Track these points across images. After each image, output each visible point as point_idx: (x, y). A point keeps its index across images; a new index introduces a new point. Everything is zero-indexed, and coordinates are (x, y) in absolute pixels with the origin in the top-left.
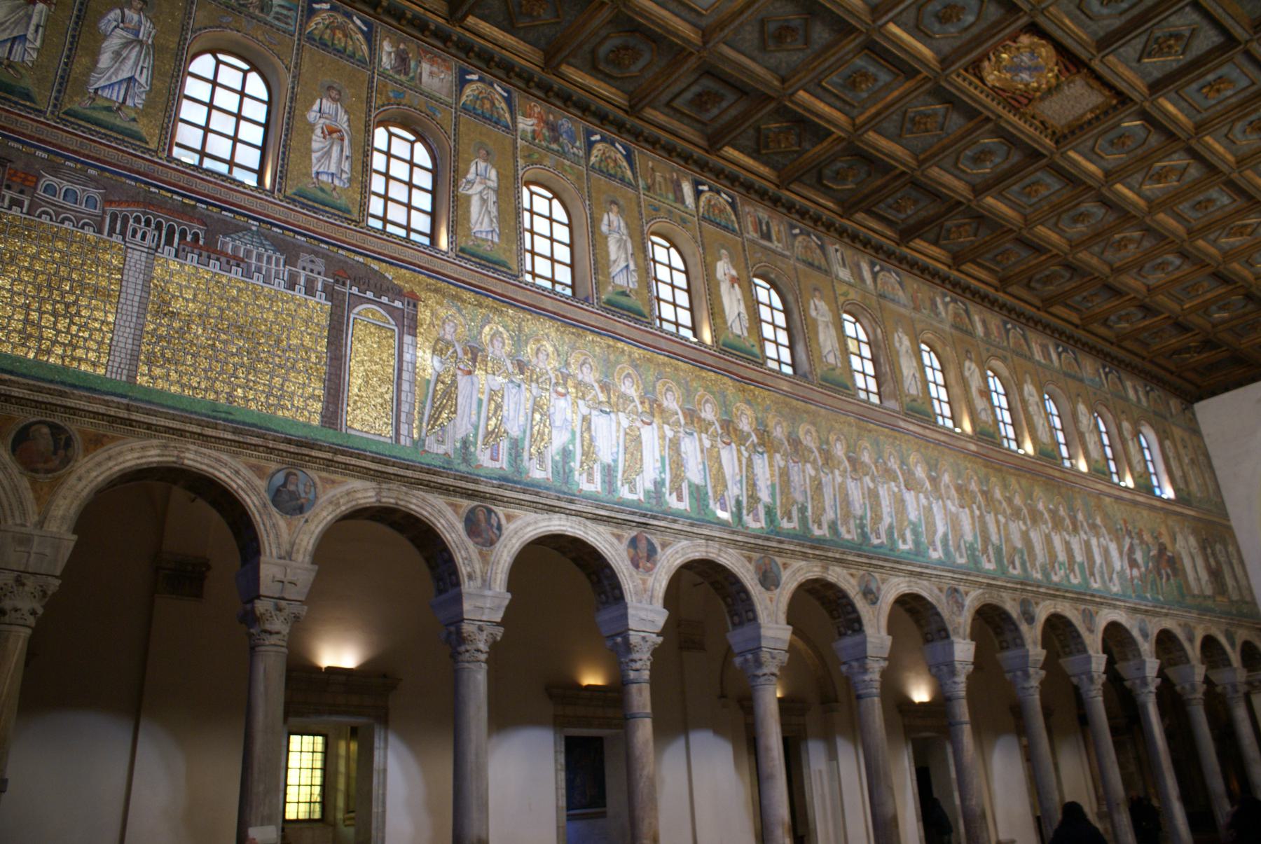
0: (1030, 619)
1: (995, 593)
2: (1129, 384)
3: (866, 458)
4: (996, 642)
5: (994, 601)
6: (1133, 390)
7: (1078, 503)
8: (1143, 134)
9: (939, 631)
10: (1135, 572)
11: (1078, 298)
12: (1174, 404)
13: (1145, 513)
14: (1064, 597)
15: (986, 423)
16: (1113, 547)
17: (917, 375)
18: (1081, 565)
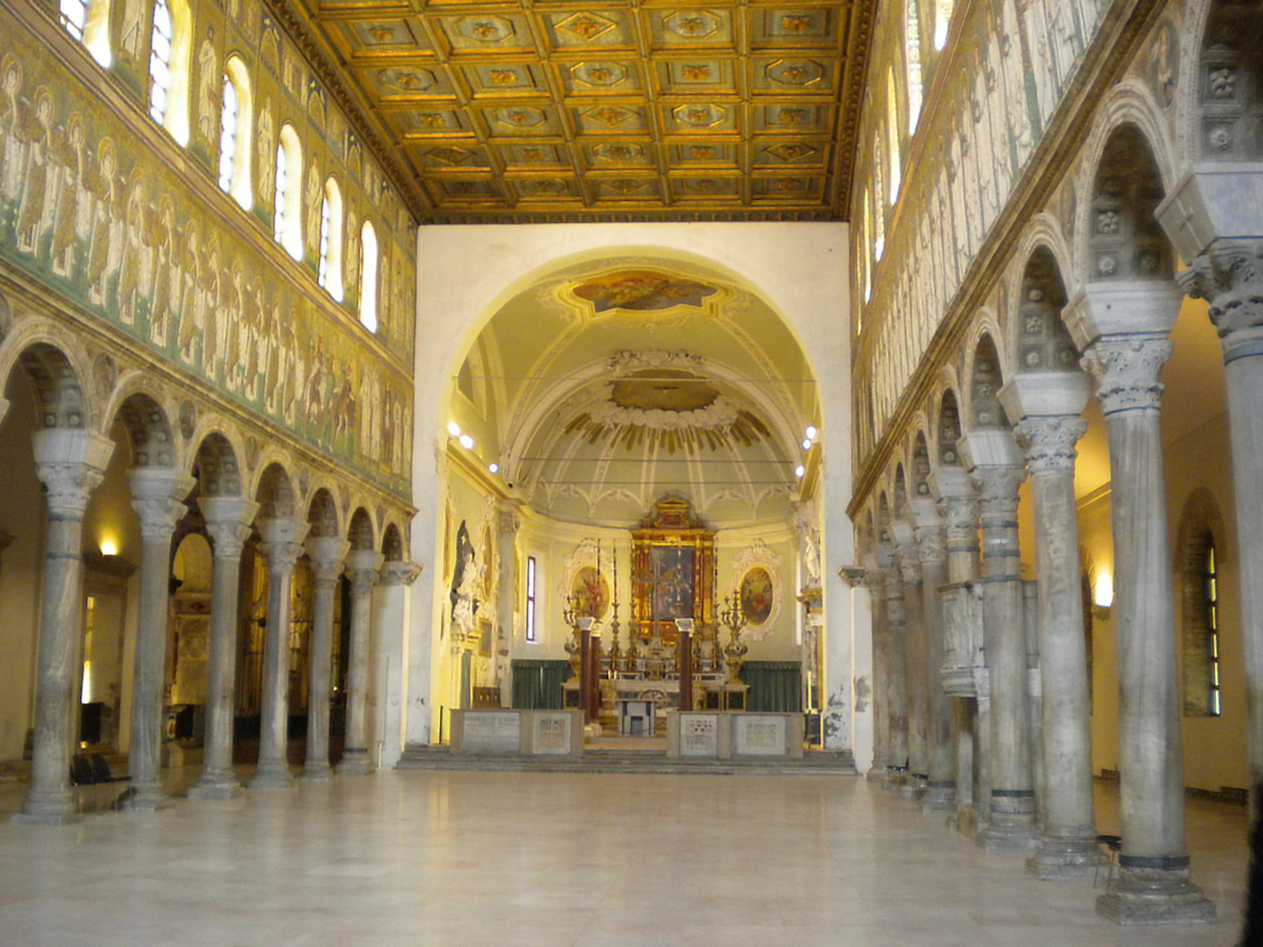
0: (188, 432)
1: (156, 380)
2: (368, 167)
3: (44, 114)
4: (131, 454)
5: (152, 393)
6: (371, 178)
7: (279, 295)
9: (69, 414)
10: (315, 408)
11: (365, 25)
12: (403, 215)
13: (342, 337)
14: (234, 414)
15: (206, 139)
16: (300, 367)
17: (142, 27)
18: (262, 377)
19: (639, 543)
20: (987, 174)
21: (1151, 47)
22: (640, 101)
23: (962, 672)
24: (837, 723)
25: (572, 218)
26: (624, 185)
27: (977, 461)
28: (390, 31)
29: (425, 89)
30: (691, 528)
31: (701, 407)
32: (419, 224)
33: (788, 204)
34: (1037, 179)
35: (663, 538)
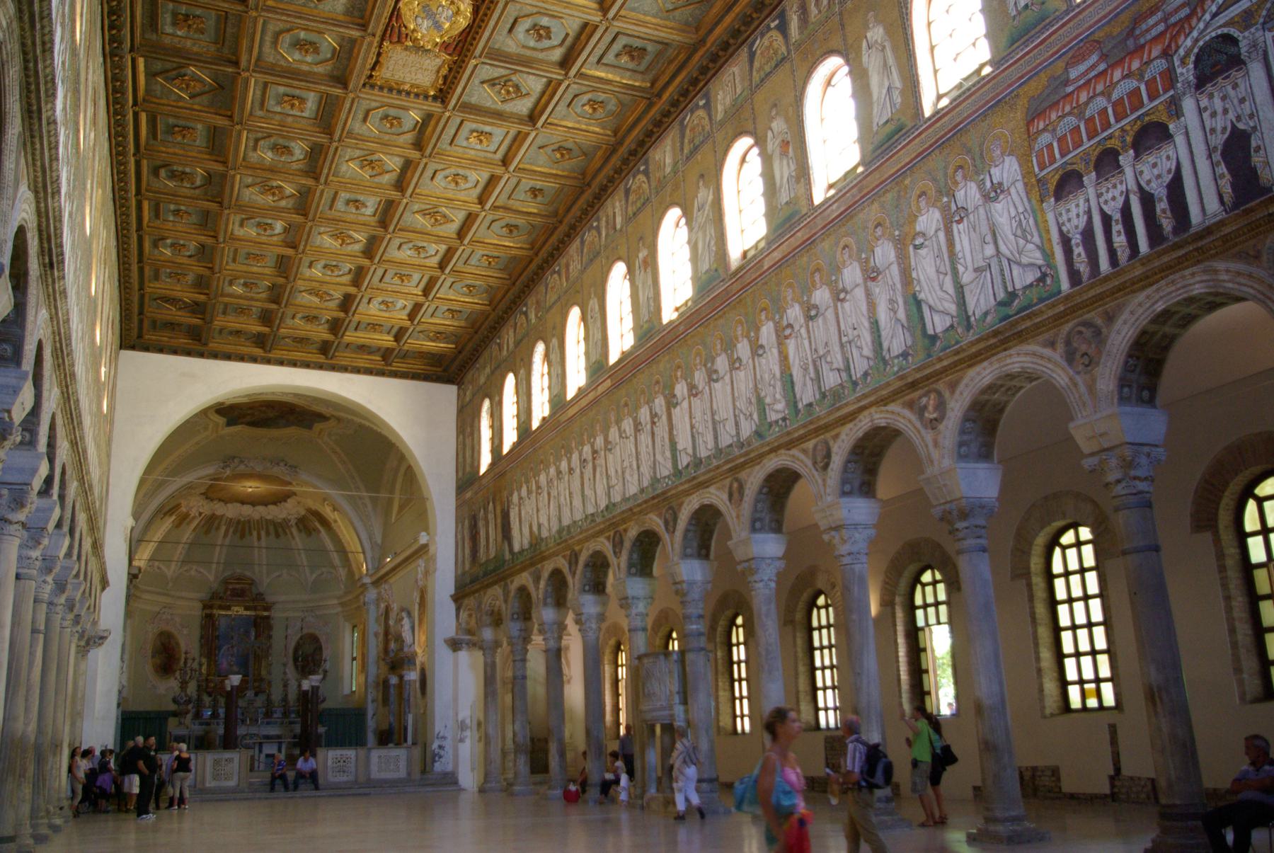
8: (408, 125)
19: (208, 611)
20: (725, 412)
21: (920, 398)
22: (352, 290)
23: (662, 708)
24: (442, 753)
25: (254, 360)
26: (302, 341)
27: (685, 578)
28: (190, 214)
29: (190, 256)
30: (253, 600)
31: (275, 503)
32: (121, 348)
33: (418, 367)
34: (796, 435)
35: (228, 608)
